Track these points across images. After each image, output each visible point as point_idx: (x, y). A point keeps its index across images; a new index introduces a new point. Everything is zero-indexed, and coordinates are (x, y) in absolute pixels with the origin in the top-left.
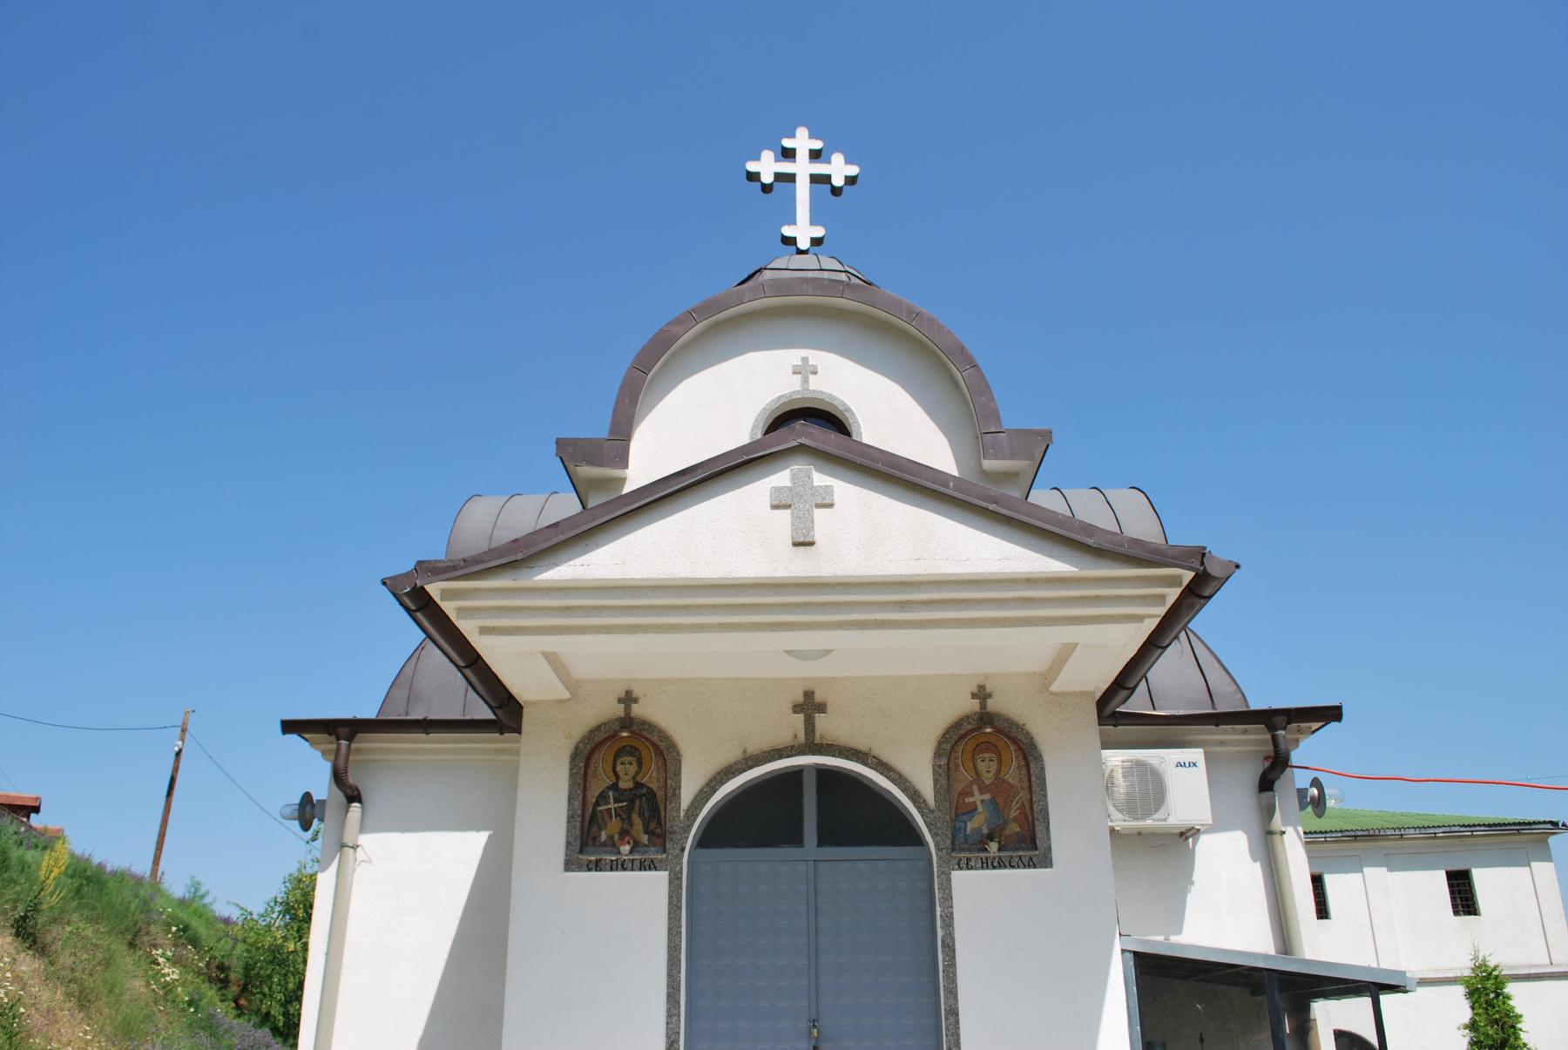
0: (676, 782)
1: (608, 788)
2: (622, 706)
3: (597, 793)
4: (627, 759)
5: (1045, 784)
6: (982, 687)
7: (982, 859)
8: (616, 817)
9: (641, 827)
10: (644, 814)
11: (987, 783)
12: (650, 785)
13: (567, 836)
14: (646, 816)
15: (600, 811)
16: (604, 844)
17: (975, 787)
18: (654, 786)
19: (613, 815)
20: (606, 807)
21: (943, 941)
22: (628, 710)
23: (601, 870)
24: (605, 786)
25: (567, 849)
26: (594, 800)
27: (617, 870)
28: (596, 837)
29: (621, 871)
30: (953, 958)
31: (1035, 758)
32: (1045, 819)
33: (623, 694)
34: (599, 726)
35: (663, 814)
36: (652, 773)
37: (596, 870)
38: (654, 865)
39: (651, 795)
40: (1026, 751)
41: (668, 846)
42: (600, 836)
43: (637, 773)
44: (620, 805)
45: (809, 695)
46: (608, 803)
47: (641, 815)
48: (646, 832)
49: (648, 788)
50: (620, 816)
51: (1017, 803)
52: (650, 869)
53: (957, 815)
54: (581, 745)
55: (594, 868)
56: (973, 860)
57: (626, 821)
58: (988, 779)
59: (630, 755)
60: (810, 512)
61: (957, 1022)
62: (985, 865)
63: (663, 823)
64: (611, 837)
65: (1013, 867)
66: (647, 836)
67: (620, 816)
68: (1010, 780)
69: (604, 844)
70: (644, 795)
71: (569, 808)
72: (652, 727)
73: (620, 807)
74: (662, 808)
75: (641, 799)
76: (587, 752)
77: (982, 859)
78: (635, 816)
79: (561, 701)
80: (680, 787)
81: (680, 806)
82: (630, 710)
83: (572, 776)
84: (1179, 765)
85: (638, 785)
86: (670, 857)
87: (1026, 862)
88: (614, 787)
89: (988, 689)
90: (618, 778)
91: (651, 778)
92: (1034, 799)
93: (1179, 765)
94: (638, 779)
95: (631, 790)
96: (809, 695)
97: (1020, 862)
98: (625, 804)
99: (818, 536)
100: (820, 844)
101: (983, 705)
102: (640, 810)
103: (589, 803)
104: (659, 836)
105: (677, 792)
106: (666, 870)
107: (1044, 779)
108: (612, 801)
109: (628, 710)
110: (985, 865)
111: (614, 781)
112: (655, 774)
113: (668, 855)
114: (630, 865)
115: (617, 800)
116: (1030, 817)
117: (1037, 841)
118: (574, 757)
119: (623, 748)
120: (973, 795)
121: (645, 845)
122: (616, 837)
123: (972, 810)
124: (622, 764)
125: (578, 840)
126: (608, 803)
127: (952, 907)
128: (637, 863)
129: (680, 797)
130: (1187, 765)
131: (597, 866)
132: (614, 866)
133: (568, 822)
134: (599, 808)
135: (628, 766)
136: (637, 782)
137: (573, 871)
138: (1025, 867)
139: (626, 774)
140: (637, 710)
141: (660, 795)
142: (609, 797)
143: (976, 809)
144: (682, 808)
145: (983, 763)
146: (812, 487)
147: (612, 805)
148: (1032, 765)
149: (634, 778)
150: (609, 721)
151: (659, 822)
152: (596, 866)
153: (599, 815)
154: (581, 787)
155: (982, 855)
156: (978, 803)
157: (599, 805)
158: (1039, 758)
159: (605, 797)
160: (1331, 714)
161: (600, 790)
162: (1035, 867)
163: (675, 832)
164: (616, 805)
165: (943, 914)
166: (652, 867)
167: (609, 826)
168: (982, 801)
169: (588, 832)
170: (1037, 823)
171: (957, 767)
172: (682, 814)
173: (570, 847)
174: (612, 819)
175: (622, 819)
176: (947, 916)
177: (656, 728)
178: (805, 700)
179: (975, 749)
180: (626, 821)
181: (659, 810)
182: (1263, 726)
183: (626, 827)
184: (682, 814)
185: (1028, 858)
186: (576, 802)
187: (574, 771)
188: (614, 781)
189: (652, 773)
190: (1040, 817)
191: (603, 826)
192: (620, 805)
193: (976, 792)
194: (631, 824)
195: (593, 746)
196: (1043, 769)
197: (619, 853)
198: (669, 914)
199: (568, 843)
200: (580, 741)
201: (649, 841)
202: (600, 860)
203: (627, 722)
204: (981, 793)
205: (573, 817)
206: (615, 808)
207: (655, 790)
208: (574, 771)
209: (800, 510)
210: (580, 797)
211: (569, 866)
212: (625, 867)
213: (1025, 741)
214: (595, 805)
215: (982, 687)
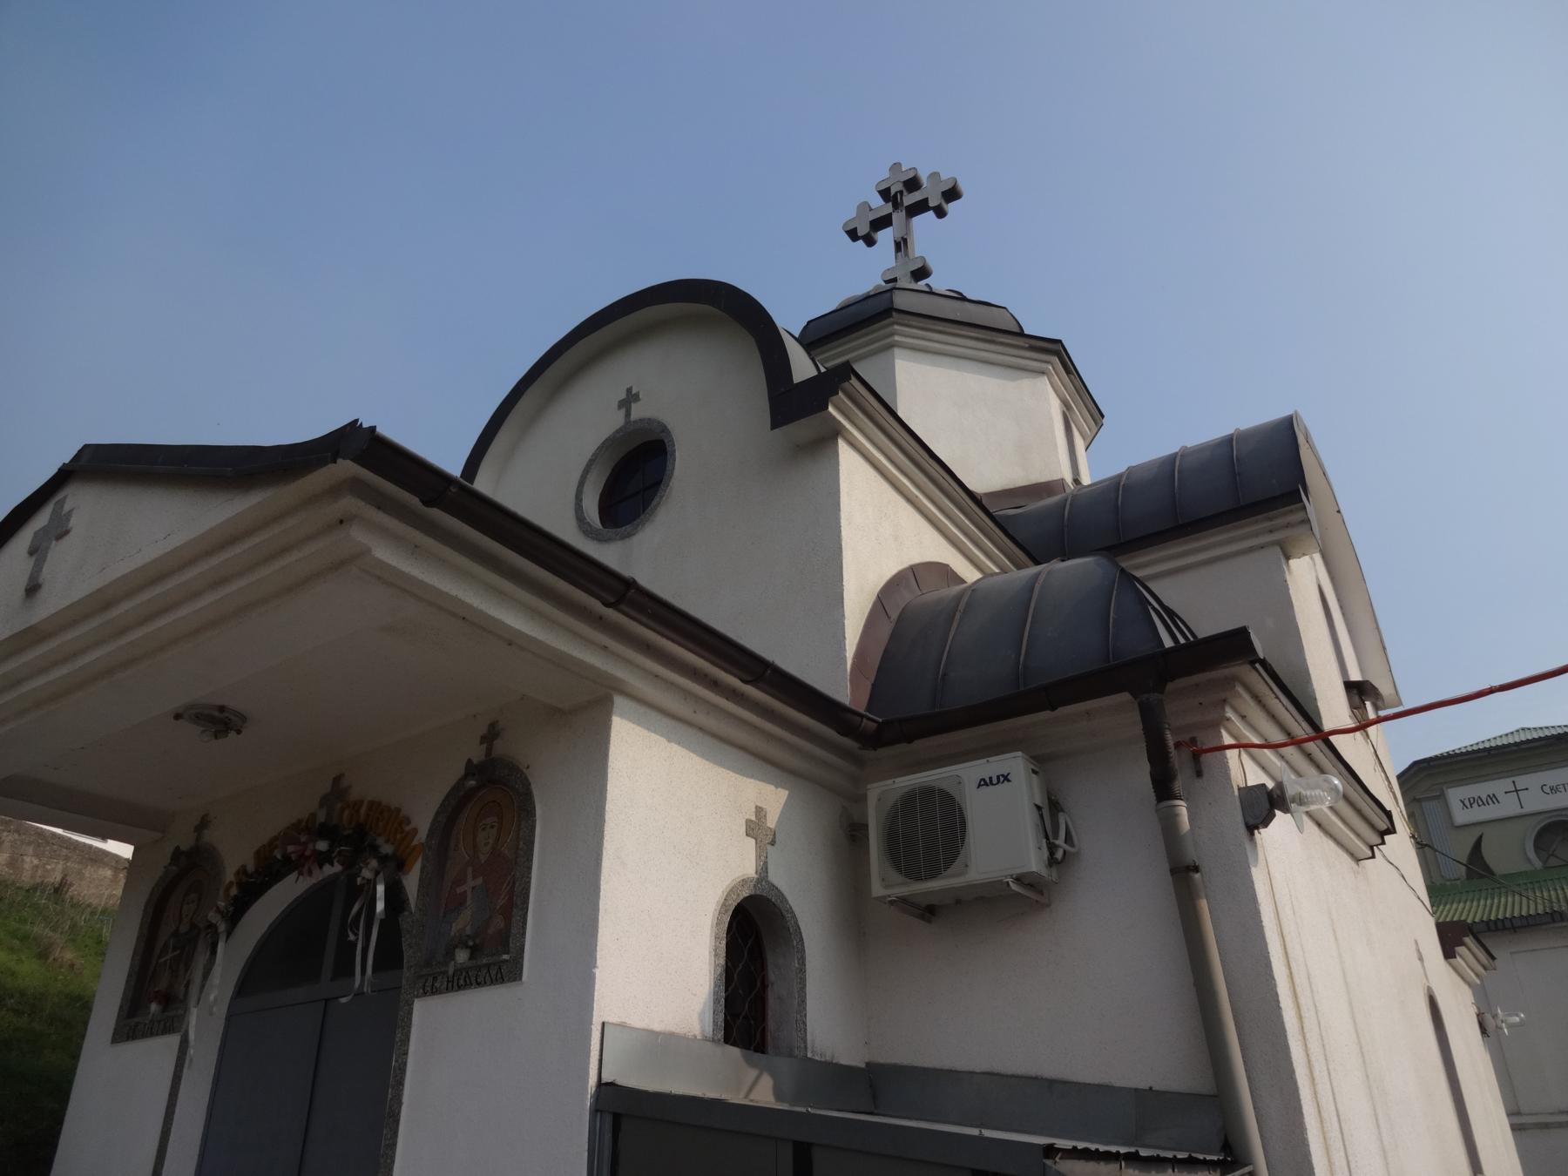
51: (508, 885)
68: (506, 852)
84: (983, 783)
87: (493, 973)
93: (983, 783)
101: (489, 751)
130: (995, 781)
176: (400, 1069)
185: (496, 967)
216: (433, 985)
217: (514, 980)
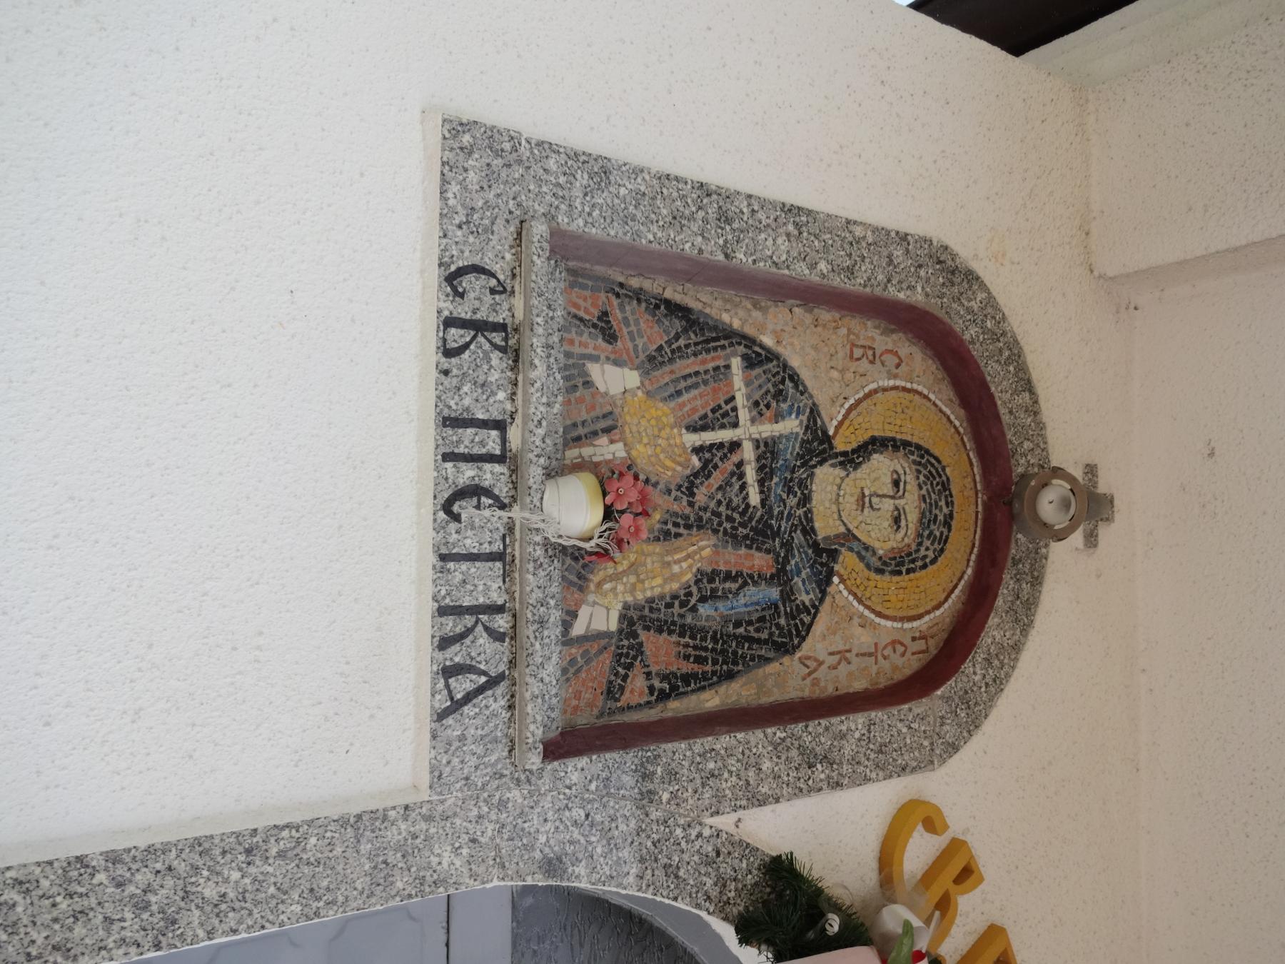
1: (814, 412)
3: (795, 362)
4: (911, 504)
8: (698, 450)
9: (655, 587)
10: (714, 596)
13: (638, 171)
15: (728, 367)
19: (709, 437)
20: (740, 400)
24: (821, 398)
25: (577, 158)
26: (768, 341)
28: (611, 337)
29: (443, 478)
34: (1029, 387)
35: (711, 700)
37: (449, 322)
38: (468, 698)
42: (617, 363)
44: (751, 474)
48: (633, 621)
49: (812, 611)
50: (705, 471)
52: (449, 672)
54: (981, 296)
55: (464, 311)
57: (682, 507)
59: (923, 514)
63: (675, 707)
66: (614, 626)
67: (705, 471)
70: (787, 595)
71: (764, 203)
75: (771, 580)
76: (958, 326)
80: (838, 785)
81: (762, 803)
90: (852, 459)
94: (847, 561)
95: (809, 531)
98: (754, 498)
102: (728, 577)
103: (757, 314)
104: (612, 692)
105: (821, 772)
106: (437, 775)
108: (767, 430)
111: (840, 445)
112: (863, 639)
114: (470, 543)
115: (767, 449)
119: (945, 486)
121: (567, 626)
122: (606, 450)
124: (896, 483)
125: (616, 232)
132: (468, 439)
134: (736, 363)
135: (888, 505)
136: (833, 555)
137: (448, 171)
139: (863, 501)
142: (778, 417)
149: (849, 537)
150: (1041, 426)
151: (674, 686)
152: (479, 327)
153: (710, 361)
154: (837, 281)
157: (751, 362)
159: (779, 395)
161: (805, 374)
164: (748, 452)
166: (462, 685)
167: (664, 411)
169: (638, 295)
172: (725, 822)
174: (693, 428)
175: (689, 487)
177: (1026, 628)
180: (682, 507)
181: (730, 676)
183: (663, 504)
184: (725, 822)
187: (898, 253)
188: (840, 445)
191: (663, 375)
192: (751, 474)
195: (976, 351)
198: (113, 858)
202: (515, 356)
205: (724, 218)
206: (735, 446)
207: (806, 646)
208: (898, 253)
210: (801, 270)
212: (466, 509)
214: (750, 341)
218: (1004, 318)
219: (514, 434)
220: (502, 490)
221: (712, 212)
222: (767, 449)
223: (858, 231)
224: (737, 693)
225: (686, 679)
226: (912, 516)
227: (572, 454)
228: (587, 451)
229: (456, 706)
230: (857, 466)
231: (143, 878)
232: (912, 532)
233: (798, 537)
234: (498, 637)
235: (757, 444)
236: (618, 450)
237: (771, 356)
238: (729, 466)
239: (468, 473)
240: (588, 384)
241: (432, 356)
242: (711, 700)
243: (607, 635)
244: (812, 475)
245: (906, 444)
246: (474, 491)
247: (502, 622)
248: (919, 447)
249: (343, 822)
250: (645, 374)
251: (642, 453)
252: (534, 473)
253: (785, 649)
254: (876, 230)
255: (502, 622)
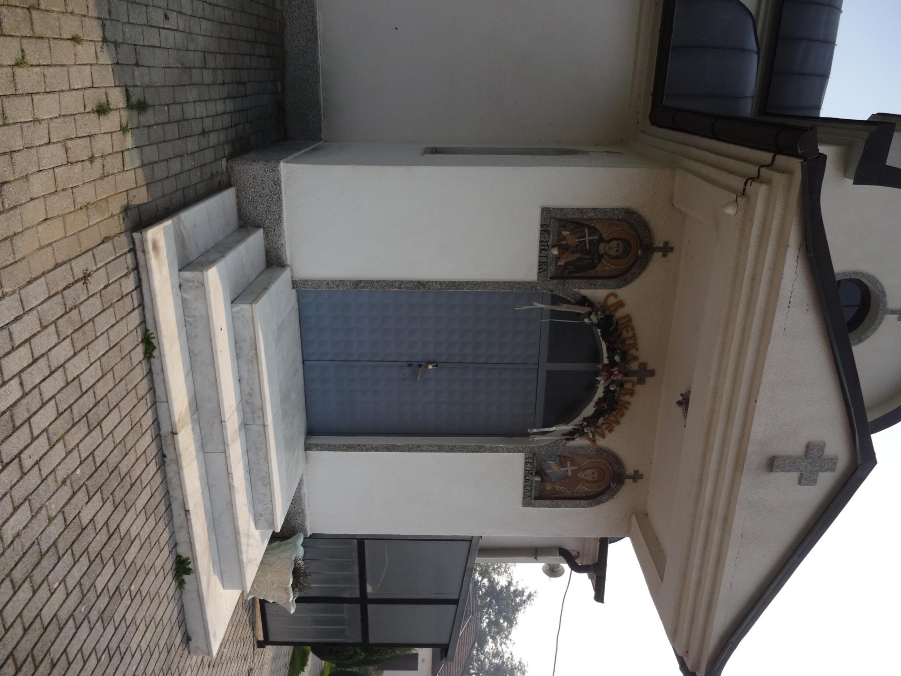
0: (599, 286)
1: (601, 235)
2: (661, 245)
3: (598, 228)
5: (574, 507)
6: (641, 477)
7: (531, 470)
8: (578, 242)
9: (570, 259)
11: (578, 474)
12: (600, 265)
14: (578, 263)
15: (585, 230)
16: (559, 233)
17: (576, 467)
18: (598, 268)
19: (580, 240)
20: (586, 234)
21: (482, 447)
22: (658, 249)
23: (541, 234)
25: (559, 209)
26: (592, 225)
27: (541, 246)
28: (565, 228)
29: (540, 248)
30: (472, 451)
31: (591, 503)
32: (553, 505)
33: (671, 245)
34: (648, 229)
35: (578, 275)
36: (608, 266)
37: (541, 231)
39: (593, 266)
40: (596, 499)
41: (555, 281)
42: (566, 231)
43: (609, 256)
44: (587, 245)
45: (652, 373)
46: (589, 236)
47: (579, 259)
49: (598, 264)
50: (579, 244)
51: (564, 490)
52: (540, 269)
53: (560, 456)
55: (543, 230)
56: (531, 466)
58: (581, 475)
60: (797, 470)
61: (435, 451)
62: (527, 472)
63: (572, 275)
64: (564, 238)
65: (525, 487)
66: (563, 264)
68: (579, 487)
69: (559, 233)
71: (589, 209)
72: (643, 268)
73: (586, 244)
74: (583, 274)
77: (531, 470)
78: (578, 255)
79: (672, 198)
80: (596, 289)
81: (582, 289)
82: (658, 251)
83: (613, 210)
85: (601, 257)
86: (547, 282)
87: (528, 493)
88: (601, 240)
89: (640, 481)
90: (608, 242)
91: (605, 266)
92: (565, 501)
96: (652, 373)
97: (527, 490)
98: (588, 248)
99: (778, 477)
100: (549, 373)
101: (629, 477)
102: (582, 259)
105: (593, 286)
106: (538, 279)
107: (577, 507)
108: (591, 238)
109: (658, 249)
110: (527, 472)
112: (608, 269)
113: (549, 281)
115: (591, 241)
116: (554, 496)
117: (539, 501)
118: (629, 212)
120: (571, 466)
123: (563, 465)
124: (618, 245)
126: (589, 236)
127: (503, 452)
128: (545, 260)
129: (588, 289)
131: (544, 230)
133: (578, 209)
134: (586, 229)
137: (542, 214)
138: (524, 493)
140: (657, 256)
141: (592, 273)
143: (563, 467)
144: (581, 290)
145: (591, 472)
146: (817, 472)
147: (587, 238)
148: (586, 501)
149: (606, 254)
155: (534, 472)
156: (566, 469)
157: (588, 229)
158: (591, 505)
160: (599, 596)
161: (599, 230)
162: (524, 498)
163: (564, 285)
164: (587, 241)
165: (499, 448)
168: (567, 471)
170: (550, 501)
171: (591, 458)
172: (577, 290)
173: (559, 211)
175: (576, 247)
178: (648, 371)
179: (601, 469)
181: (581, 272)
182: (597, 561)
184: (577, 290)
185: (530, 495)
186: (592, 214)
187: (616, 212)
189: (608, 266)
190: (553, 503)
192: (587, 245)
193: (573, 468)
194: (572, 253)
196: (583, 507)
197: (553, 247)
198: (508, 282)
199: (562, 210)
200: (638, 215)
201: (559, 265)
202: (549, 234)
203: (649, 249)
204: (572, 471)
205: (581, 212)
206: (585, 241)
207: (596, 269)
208: (616, 212)
209: (800, 463)
211: (547, 213)
212: (543, 252)
213: (602, 499)
214: (590, 225)
215: (641, 477)
216: (529, 462)
217: (523, 504)
218: (642, 218)
219: (549, 243)
220: (547, 249)
221: (579, 212)
222: (591, 241)
223: (607, 210)
224: (583, 274)
225: (574, 272)
226: (621, 250)
227: (558, 243)
228: (561, 243)
229: (540, 272)
230: (609, 243)
231: (510, 284)
232: (621, 252)
233: (596, 253)
234: (545, 265)
235: (589, 240)
236: (566, 242)
237: (593, 227)
238: (584, 243)
239: (543, 247)
240: (561, 234)
241: (539, 235)
242: (578, 275)
243: (562, 265)
244: (599, 244)
245: (621, 239)
246: (543, 249)
247: (546, 264)
248: (624, 239)
249: (528, 282)
250: (570, 232)
251: (569, 242)
252: (550, 248)
253: (592, 269)
254: (611, 209)
255: (546, 264)
